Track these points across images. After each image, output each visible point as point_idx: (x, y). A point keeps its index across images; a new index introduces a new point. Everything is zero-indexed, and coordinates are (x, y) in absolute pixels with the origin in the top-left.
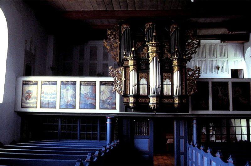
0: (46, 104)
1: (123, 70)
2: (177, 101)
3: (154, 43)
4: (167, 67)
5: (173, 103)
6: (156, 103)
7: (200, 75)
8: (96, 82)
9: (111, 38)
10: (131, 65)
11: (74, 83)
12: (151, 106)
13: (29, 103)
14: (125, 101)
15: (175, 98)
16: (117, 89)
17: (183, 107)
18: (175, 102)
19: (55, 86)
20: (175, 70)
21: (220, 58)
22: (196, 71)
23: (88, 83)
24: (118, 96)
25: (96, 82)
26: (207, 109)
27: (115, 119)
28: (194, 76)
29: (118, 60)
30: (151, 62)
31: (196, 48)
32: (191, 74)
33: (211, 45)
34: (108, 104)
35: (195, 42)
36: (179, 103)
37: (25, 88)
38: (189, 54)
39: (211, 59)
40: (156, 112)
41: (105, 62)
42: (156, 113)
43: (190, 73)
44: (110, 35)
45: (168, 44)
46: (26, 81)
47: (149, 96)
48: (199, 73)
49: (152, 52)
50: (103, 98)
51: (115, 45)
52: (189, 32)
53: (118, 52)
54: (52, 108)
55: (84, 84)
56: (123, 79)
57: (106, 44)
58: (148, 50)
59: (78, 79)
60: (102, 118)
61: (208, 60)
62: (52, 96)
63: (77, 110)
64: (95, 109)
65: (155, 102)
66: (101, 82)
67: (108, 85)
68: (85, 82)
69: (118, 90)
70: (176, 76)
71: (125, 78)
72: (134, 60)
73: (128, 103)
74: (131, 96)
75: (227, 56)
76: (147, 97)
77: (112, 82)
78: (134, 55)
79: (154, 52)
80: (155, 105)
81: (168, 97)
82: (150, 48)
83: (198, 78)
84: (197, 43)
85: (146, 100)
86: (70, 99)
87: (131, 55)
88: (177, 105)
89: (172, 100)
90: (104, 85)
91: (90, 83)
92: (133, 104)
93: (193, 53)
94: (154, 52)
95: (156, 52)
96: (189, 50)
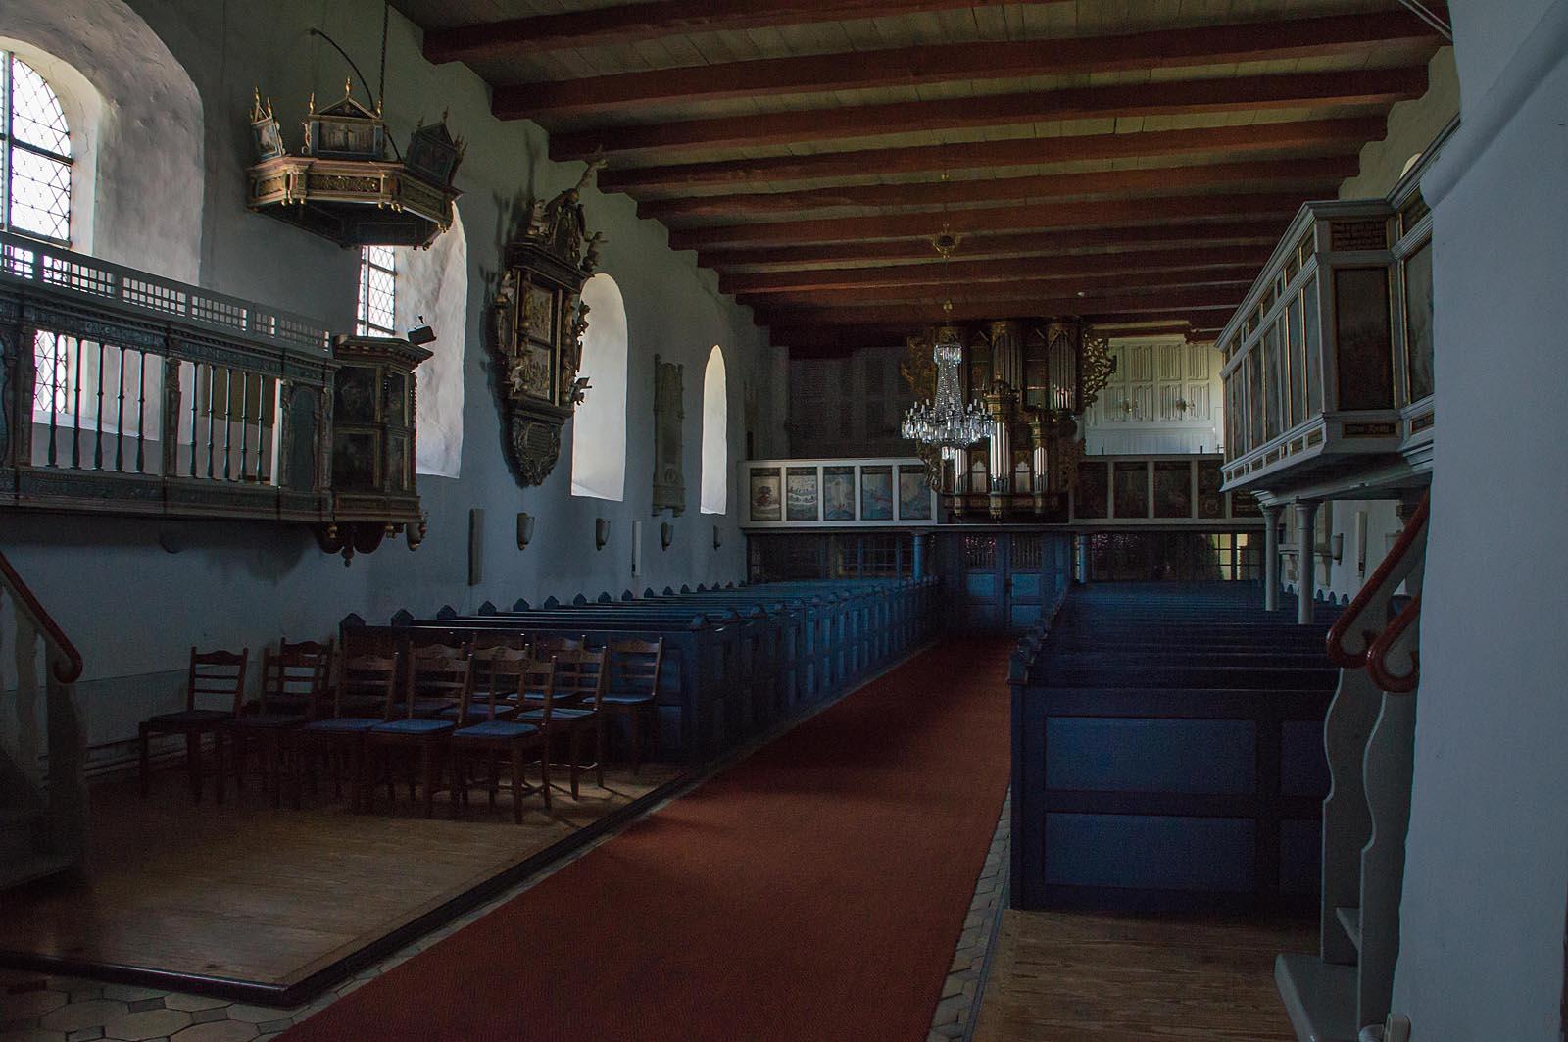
0: (798, 511)
2: (1039, 503)
5: (1034, 506)
11: (850, 470)
13: (763, 512)
17: (1055, 513)
19: (813, 477)
21: (1189, 380)
24: (934, 495)
27: (928, 536)
31: (1107, 375)
37: (756, 482)
38: (1091, 388)
46: (756, 469)
54: (810, 519)
59: (857, 463)
60: (904, 536)
61: (1158, 385)
62: (809, 497)
63: (858, 523)
66: (900, 467)
70: (1039, 454)
73: (952, 507)
74: (957, 496)
75: (1206, 374)
76: (985, 497)
81: (1024, 495)
86: (843, 500)
96: (1091, 381)
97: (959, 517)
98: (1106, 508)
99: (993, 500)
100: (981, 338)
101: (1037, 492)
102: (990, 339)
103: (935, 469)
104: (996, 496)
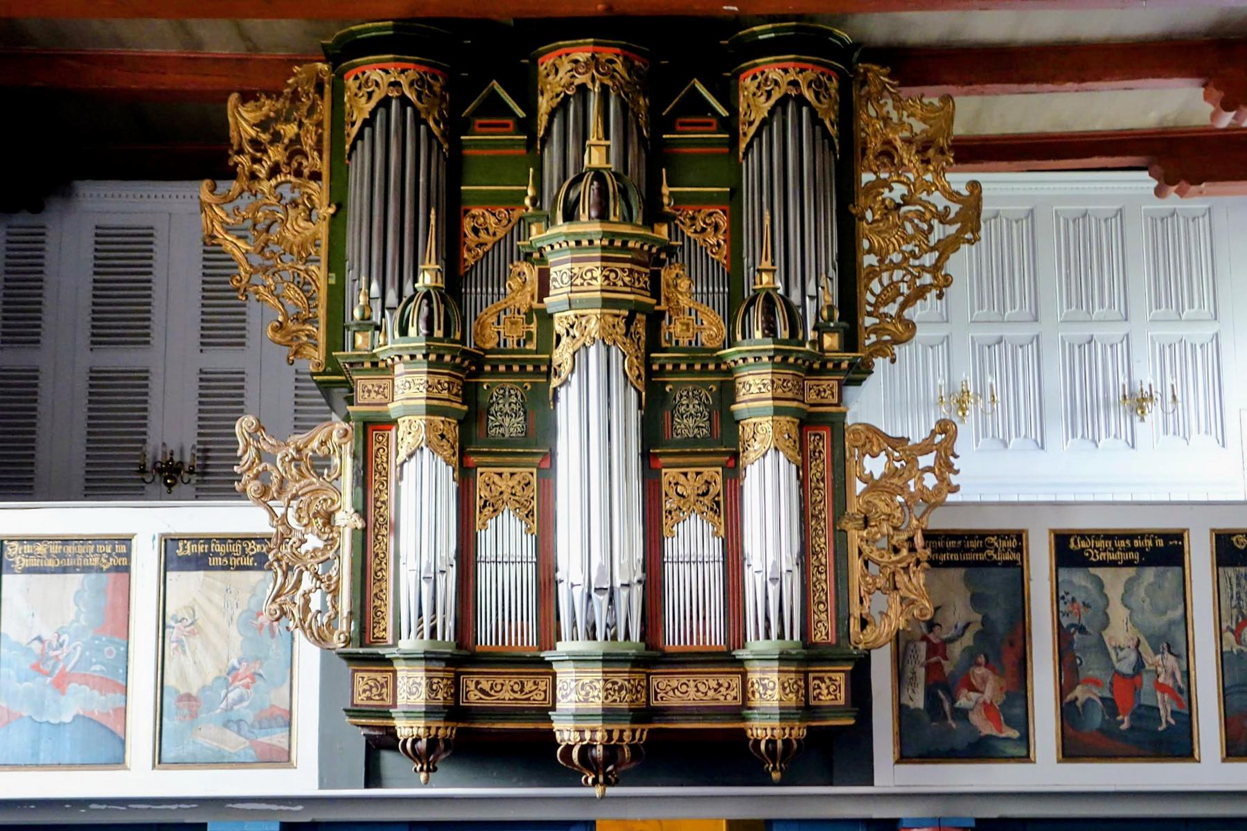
1: (347, 448)
3: (585, 234)
4: (691, 422)
6: (608, 714)
7: (954, 480)
8: (127, 540)
9: (262, 172)
10: (409, 411)
12: (565, 732)
14: (360, 699)
15: (757, 666)
16: (299, 600)
18: (756, 702)
20: (757, 446)
22: (924, 448)
23: (62, 556)
24: (308, 656)
25: (127, 540)
26: (1023, 754)
28: (903, 489)
29: (319, 355)
30: (566, 382)
31: (947, 247)
32: (884, 476)
33: (1085, 215)
34: (226, 724)
35: (938, 200)
36: (785, 714)
39: (1081, 332)
40: (607, 783)
41: (222, 360)
42: (611, 791)
43: (876, 466)
44: (255, 143)
45: (724, 225)
47: (547, 655)
48: (945, 466)
49: (570, 304)
50: (183, 676)
51: (297, 228)
52: (894, 115)
53: (322, 284)
55: (26, 563)
56: (347, 519)
57: (223, 222)
58: (544, 290)
64: (118, 762)
65: (597, 704)
66: (169, 542)
67: (226, 568)
68: (41, 548)
69: (306, 608)
71: (363, 513)
72: (430, 364)
74: (409, 658)
77: (262, 539)
78: (430, 327)
79: (588, 304)
80: (593, 731)
82: (560, 272)
83: (942, 503)
84: (955, 208)
85: (529, 686)
87: (412, 331)
88: (768, 724)
89: (736, 681)
90: (198, 569)
91: (81, 550)
92: (422, 723)
93: (920, 293)
94: (588, 304)
95: (606, 303)
96: (898, 266)
97: (416, 756)
98: (1023, 724)
99: (566, 676)
100: (495, 107)
101: (756, 645)
102: (532, 110)
103: (313, 542)
104: (579, 660)
